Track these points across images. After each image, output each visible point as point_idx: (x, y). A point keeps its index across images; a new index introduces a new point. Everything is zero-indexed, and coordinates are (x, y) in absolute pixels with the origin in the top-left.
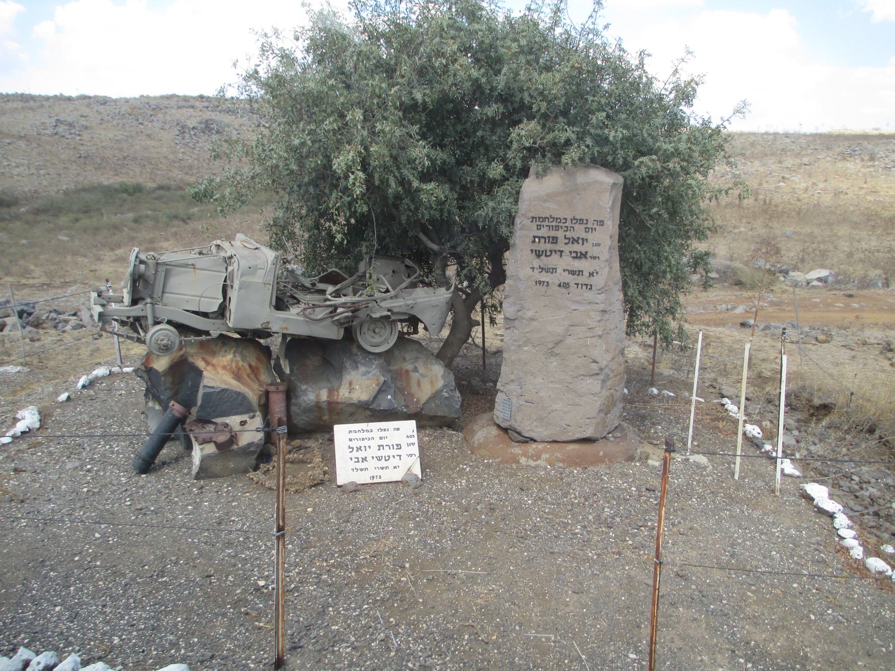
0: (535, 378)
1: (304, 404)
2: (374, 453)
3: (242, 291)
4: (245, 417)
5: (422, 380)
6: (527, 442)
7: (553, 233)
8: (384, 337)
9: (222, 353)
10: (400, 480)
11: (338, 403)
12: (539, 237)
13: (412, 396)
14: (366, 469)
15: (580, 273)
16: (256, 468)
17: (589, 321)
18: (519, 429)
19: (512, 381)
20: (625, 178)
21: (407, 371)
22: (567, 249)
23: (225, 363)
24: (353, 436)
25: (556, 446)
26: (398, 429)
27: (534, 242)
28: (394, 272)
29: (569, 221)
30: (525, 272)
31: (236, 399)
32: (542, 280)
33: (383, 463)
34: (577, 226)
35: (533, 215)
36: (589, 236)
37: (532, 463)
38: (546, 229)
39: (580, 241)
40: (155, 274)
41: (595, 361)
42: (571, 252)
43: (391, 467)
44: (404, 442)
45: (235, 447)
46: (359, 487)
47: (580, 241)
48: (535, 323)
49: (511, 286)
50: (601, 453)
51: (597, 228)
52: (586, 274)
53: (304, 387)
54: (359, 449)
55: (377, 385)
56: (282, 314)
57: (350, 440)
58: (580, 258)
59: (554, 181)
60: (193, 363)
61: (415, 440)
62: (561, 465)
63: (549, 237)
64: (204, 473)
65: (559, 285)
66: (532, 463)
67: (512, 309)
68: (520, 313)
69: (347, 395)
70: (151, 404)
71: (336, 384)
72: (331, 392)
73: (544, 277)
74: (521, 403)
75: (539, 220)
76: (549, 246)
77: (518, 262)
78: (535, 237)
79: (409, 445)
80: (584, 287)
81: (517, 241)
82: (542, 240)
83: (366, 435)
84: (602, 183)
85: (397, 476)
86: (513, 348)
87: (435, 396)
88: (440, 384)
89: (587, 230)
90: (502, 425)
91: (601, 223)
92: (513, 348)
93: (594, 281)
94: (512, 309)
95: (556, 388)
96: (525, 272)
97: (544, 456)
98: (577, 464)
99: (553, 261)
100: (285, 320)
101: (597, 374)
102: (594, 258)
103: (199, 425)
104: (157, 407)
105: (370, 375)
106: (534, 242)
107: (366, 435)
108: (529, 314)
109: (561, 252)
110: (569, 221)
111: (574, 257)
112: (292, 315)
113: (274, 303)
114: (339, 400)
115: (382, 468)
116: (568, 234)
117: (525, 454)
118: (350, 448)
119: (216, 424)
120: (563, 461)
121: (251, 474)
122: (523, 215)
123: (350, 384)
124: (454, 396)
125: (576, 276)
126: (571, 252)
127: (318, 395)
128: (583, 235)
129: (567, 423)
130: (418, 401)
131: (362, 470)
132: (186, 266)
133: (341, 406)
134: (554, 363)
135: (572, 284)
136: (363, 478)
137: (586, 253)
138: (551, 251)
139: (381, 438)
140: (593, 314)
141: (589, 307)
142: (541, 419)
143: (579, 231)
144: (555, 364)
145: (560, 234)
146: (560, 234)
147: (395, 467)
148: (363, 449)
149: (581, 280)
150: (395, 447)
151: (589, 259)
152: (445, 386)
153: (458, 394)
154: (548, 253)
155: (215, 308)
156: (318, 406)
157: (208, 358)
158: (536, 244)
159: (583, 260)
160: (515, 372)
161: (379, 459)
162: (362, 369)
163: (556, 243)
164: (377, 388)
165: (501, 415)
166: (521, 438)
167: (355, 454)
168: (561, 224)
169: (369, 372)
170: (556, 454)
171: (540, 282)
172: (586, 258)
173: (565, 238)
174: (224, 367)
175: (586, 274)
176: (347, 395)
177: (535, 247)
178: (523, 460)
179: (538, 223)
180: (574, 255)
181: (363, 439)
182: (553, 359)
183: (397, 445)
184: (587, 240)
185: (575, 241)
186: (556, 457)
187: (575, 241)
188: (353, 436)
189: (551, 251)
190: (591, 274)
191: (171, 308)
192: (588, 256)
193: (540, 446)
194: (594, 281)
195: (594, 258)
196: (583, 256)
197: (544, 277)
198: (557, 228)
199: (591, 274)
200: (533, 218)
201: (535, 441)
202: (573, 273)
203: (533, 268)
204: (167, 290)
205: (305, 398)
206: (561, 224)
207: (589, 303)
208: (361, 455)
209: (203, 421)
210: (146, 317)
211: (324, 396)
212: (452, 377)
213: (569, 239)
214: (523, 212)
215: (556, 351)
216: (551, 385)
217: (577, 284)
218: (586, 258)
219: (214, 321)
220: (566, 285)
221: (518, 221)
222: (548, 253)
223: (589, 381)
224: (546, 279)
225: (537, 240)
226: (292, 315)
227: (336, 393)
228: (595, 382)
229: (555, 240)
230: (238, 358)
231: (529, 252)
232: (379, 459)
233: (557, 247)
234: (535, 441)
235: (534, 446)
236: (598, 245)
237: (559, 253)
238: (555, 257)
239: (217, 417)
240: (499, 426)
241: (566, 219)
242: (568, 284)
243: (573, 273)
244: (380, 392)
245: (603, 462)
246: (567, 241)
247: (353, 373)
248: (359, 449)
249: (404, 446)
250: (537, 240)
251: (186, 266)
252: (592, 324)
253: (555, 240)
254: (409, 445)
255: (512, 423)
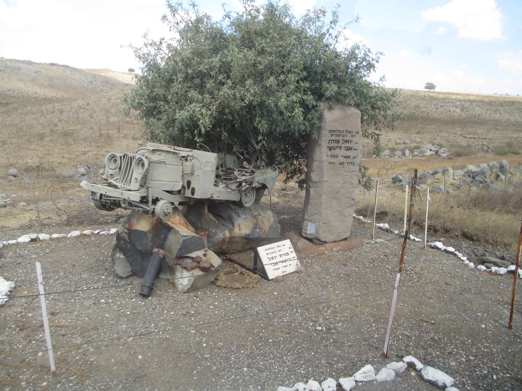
7: (337, 138)
12: (332, 140)
14: (279, 268)
15: (349, 157)
19: (315, 214)
22: (343, 146)
25: (336, 243)
26: (284, 245)
27: (329, 142)
34: (348, 135)
36: (353, 139)
41: (353, 200)
44: (289, 251)
52: (352, 157)
54: (272, 258)
55: (253, 224)
57: (267, 254)
60: (166, 223)
64: (193, 288)
65: (340, 164)
67: (317, 177)
68: (321, 179)
69: (239, 232)
72: (230, 233)
73: (333, 160)
75: (332, 132)
76: (335, 145)
77: (322, 154)
78: (330, 140)
85: (291, 269)
87: (271, 227)
90: (309, 237)
91: (358, 133)
92: (316, 197)
96: (325, 158)
99: (337, 152)
102: (355, 150)
104: (122, 256)
105: (247, 219)
106: (329, 142)
109: (341, 147)
114: (236, 236)
115: (285, 267)
117: (327, 250)
123: (239, 226)
127: (224, 234)
128: (350, 139)
130: (265, 231)
134: (334, 202)
139: (279, 251)
143: (349, 137)
145: (340, 138)
146: (340, 138)
149: (349, 160)
152: (274, 221)
159: (350, 151)
161: (282, 262)
165: (308, 232)
175: (352, 157)
176: (239, 232)
177: (330, 145)
180: (346, 148)
185: (347, 141)
187: (347, 141)
193: (331, 244)
195: (355, 150)
198: (339, 136)
199: (354, 158)
202: (345, 157)
203: (328, 156)
205: (218, 237)
208: (274, 261)
209: (180, 257)
211: (227, 234)
216: (333, 214)
220: (342, 164)
229: (338, 141)
232: (282, 262)
233: (339, 145)
235: (328, 245)
236: (357, 143)
238: (338, 150)
239: (191, 251)
243: (345, 157)
253: (338, 141)
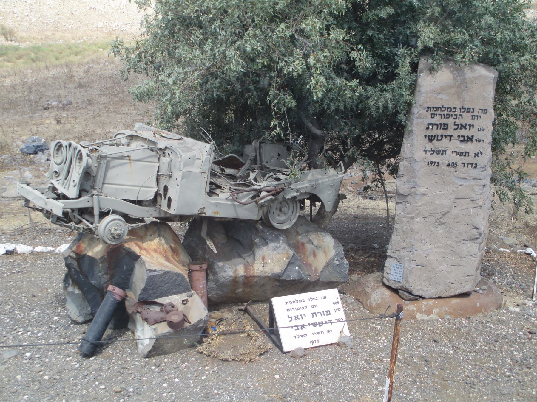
0: (424, 244)
1: (222, 280)
2: (309, 320)
3: (184, 180)
4: (184, 296)
5: (316, 251)
6: (416, 300)
7: (444, 121)
8: (288, 216)
9: (148, 237)
10: (335, 341)
11: (254, 277)
12: (433, 125)
13: (310, 265)
14: (306, 335)
15: (467, 153)
16: (200, 342)
17: (473, 195)
18: (410, 289)
19: (404, 248)
20: (500, 72)
21: (303, 244)
22: (456, 134)
23: (155, 247)
24: (289, 306)
26: (325, 297)
27: (428, 128)
28: (279, 155)
29: (458, 110)
30: (419, 154)
31: (176, 280)
32: (434, 161)
33: (318, 329)
34: (464, 114)
35: (428, 105)
36: (475, 122)
37: (425, 317)
38: (439, 117)
39: (468, 127)
40: (98, 168)
41: (476, 228)
42: (459, 136)
43: (325, 332)
44: (332, 308)
45: (187, 325)
46: (306, 352)
47: (468, 127)
48: (426, 198)
49: (405, 167)
50: (478, 305)
51: (482, 115)
52: (472, 154)
53: (220, 264)
54: (297, 317)
55: (287, 258)
56: (214, 200)
57: (288, 310)
58: (467, 141)
59: (444, 75)
60: (130, 249)
61: (340, 306)
62: (449, 317)
63: (441, 124)
64: (157, 350)
65: (449, 165)
66: (425, 317)
67: (406, 186)
68: (413, 190)
69: (261, 269)
70: (70, 289)
71: (250, 260)
72: (246, 268)
73: (435, 158)
74: (413, 266)
75: (433, 110)
76: (440, 132)
77: (415, 147)
78: (429, 124)
79: (336, 310)
80: (470, 166)
81: (413, 128)
82: (435, 127)
83: (300, 305)
84: (486, 77)
85: (333, 338)
86: (405, 220)
87: (329, 264)
88: (332, 253)
89: (473, 117)
90: (393, 286)
91: (485, 111)
92: (405, 220)
93: (477, 160)
94: (406, 186)
95: (442, 252)
96: (419, 154)
97: (435, 311)
98: (462, 315)
99: (444, 143)
100: (217, 205)
101: (477, 238)
102: (479, 141)
103: (144, 306)
104: (77, 291)
105: (279, 250)
106: (428, 128)
107: (300, 305)
108: (422, 190)
109: (451, 136)
110: (458, 110)
111: (461, 141)
112: (222, 200)
113: (208, 191)
114: (255, 274)
115: (319, 333)
116: (458, 121)
117: (419, 311)
118: (289, 317)
119: (161, 305)
120: (450, 314)
121: (200, 348)
122: (420, 105)
123: (263, 258)
124: (343, 263)
125: (462, 157)
126: (459, 136)
127: (236, 271)
128: (470, 122)
129: (450, 281)
130: (316, 270)
131: (302, 336)
132: (122, 158)
133: (255, 280)
134: (440, 230)
135: (459, 164)
136: (305, 343)
137: (473, 137)
138: (442, 136)
139: (313, 307)
140: (476, 189)
141: (473, 182)
142: (429, 279)
143: (466, 119)
144: (441, 231)
145: (450, 121)
146: (450, 121)
147: (328, 332)
148: (300, 317)
149: (467, 160)
150: (326, 313)
151: (474, 142)
152: (336, 255)
153: (346, 261)
154: (440, 138)
155: (151, 196)
156: (235, 281)
157: (140, 243)
158: (430, 130)
159: (470, 143)
160: (407, 240)
161: (315, 325)
162: (272, 245)
163: (447, 129)
164: (287, 261)
165: (392, 278)
166: (412, 297)
167: (294, 323)
168: (451, 113)
169: (278, 247)
170: (444, 308)
171: (432, 163)
172: (472, 141)
173: (455, 125)
174: (155, 251)
175: (472, 154)
176: (261, 269)
177: (429, 133)
178: (419, 316)
179: (432, 112)
180: (462, 139)
181: (298, 309)
182: (440, 227)
183: (327, 311)
184: (473, 126)
185: (463, 127)
186: (445, 311)
187: (463, 127)
188: (289, 306)
189: (442, 136)
190: (476, 155)
191: (112, 198)
192: (474, 139)
193: (430, 302)
194: (477, 160)
195: (479, 141)
196: (470, 139)
197: (435, 158)
198: (448, 116)
199: (476, 155)
200: (428, 108)
201: (423, 298)
202: (460, 154)
203: (426, 151)
204: (106, 182)
205: (224, 274)
206: (451, 113)
207: (473, 179)
208: (299, 322)
209: (146, 302)
210: (92, 208)
211: (241, 271)
212: (341, 248)
213: (458, 125)
214: (421, 103)
215: (443, 221)
216: (438, 250)
217: (464, 164)
218: (472, 141)
219: (147, 208)
220: (454, 165)
221: (415, 110)
222: (440, 138)
223: (469, 244)
224: (437, 161)
225: (431, 127)
226: (222, 200)
227: (251, 267)
228: (474, 245)
229: (445, 126)
230: (163, 241)
231: (423, 137)
232: (315, 325)
233: (448, 133)
234: (423, 298)
235: (424, 302)
236: (483, 130)
237: (449, 138)
238: (445, 141)
240: (389, 287)
241: (455, 108)
242: (456, 163)
243: (460, 154)
244: (289, 264)
245: (481, 311)
246: (456, 127)
247: (265, 248)
248: (297, 317)
249: (332, 312)
250: (431, 127)
251: (122, 158)
252: (475, 196)
253: (445, 126)
254: (336, 310)
255: (404, 284)
